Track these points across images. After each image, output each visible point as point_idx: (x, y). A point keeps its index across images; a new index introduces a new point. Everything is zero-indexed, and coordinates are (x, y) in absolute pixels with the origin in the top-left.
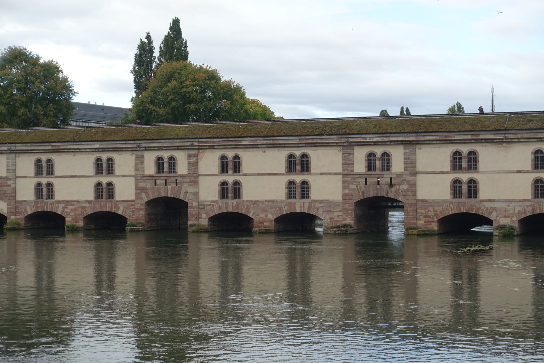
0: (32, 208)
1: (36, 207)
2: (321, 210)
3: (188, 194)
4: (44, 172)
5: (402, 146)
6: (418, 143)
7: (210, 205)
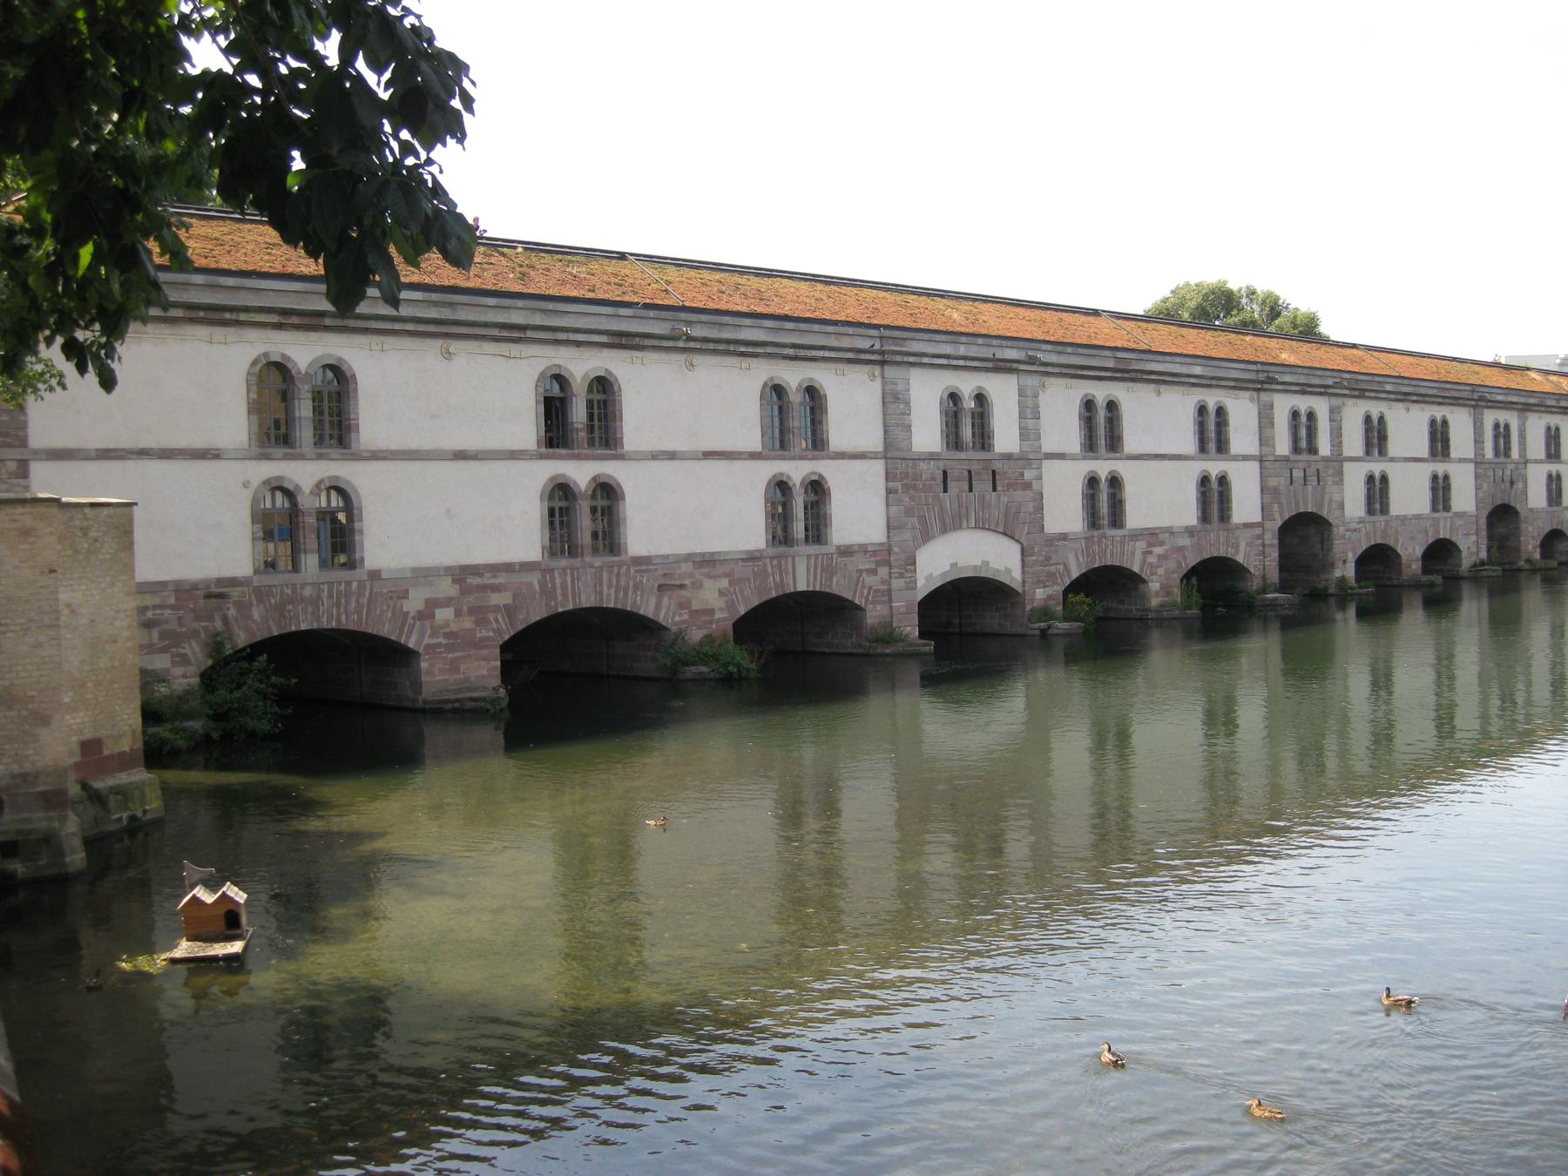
0: (1081, 559)
1: (1088, 555)
2: (1460, 532)
3: (1334, 503)
4: (1102, 443)
5: (1515, 414)
7: (1355, 530)
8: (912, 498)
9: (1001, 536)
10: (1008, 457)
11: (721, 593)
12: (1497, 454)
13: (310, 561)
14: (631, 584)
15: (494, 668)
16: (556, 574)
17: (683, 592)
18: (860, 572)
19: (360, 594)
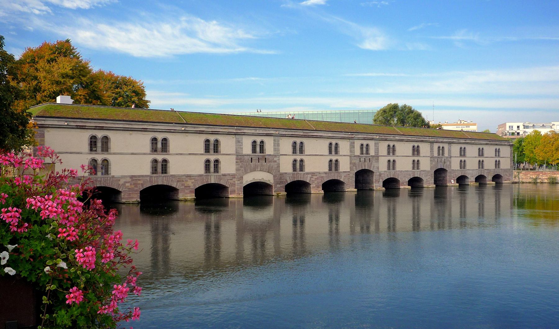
0: (291, 178)
6: (453, 143)
7: (383, 174)
8: (242, 164)
9: (267, 173)
10: (270, 155)
11: (192, 183)
12: (439, 155)
13: (99, 174)
14: (170, 180)
15: (138, 195)
16: (153, 177)
17: (183, 182)
18: (228, 179)
19: (110, 180)
